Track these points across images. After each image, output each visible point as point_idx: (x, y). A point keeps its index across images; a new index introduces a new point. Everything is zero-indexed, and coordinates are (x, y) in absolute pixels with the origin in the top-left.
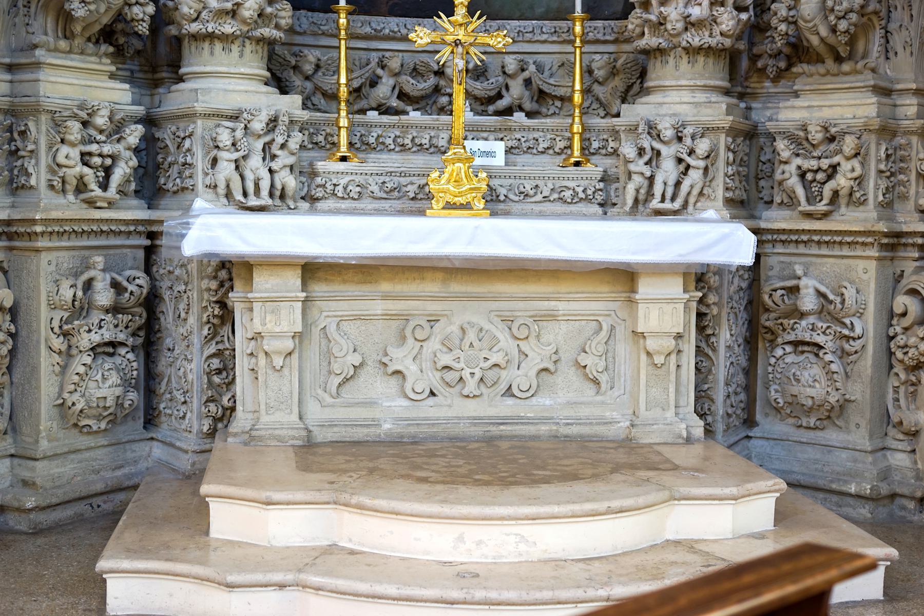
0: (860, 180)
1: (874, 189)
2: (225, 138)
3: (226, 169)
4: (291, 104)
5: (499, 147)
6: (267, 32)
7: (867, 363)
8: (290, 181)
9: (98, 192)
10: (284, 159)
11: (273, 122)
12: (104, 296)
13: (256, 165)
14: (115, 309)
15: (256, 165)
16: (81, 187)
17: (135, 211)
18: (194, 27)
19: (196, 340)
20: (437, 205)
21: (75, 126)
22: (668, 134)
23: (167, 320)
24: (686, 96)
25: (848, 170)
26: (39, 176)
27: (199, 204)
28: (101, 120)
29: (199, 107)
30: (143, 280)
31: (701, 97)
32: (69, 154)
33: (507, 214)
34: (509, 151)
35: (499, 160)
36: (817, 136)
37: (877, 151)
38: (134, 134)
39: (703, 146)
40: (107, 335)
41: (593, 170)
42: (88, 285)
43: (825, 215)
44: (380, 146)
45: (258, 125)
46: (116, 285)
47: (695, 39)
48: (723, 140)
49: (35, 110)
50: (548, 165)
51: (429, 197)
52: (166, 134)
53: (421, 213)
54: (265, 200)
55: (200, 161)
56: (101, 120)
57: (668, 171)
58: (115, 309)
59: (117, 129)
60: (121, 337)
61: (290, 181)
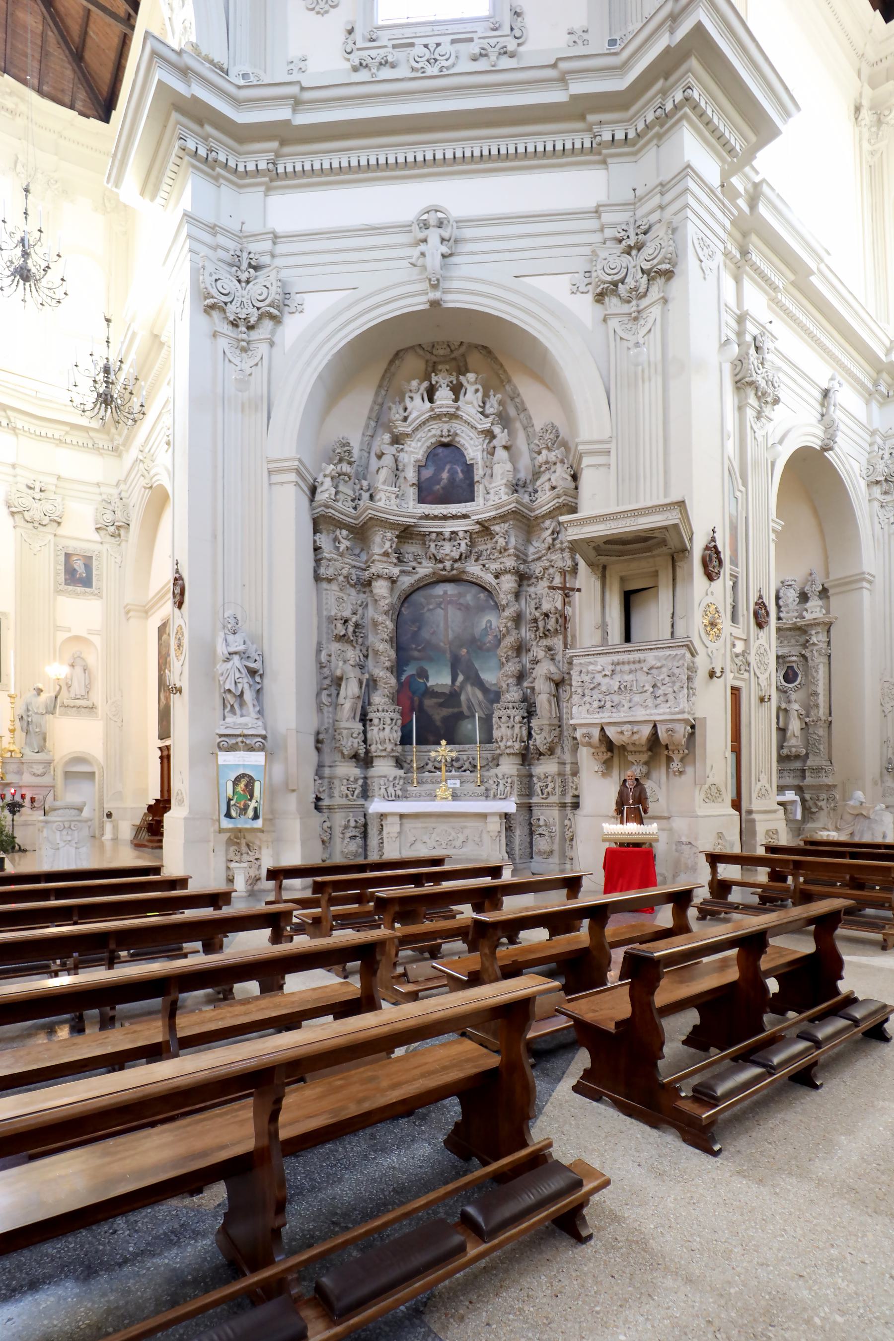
0: (554, 789)
1: (558, 791)
2: (382, 783)
3: (383, 791)
4: (401, 772)
5: (458, 782)
6: (394, 754)
7: (557, 840)
8: (399, 793)
9: (350, 797)
10: (399, 787)
11: (395, 778)
12: (352, 824)
13: (391, 790)
14: (355, 827)
15: (391, 790)
16: (347, 796)
17: (361, 801)
18: (375, 754)
19: (376, 835)
20: (438, 798)
21: (345, 781)
22: (501, 777)
23: (369, 830)
24: (507, 767)
25: (551, 785)
26: (336, 793)
27: (376, 799)
28: (352, 779)
29: (376, 774)
30: (363, 820)
31: (511, 766)
32: (344, 788)
33: (460, 800)
34: (461, 783)
35: (458, 785)
36: (543, 777)
37: (558, 780)
38: (360, 782)
39: (509, 780)
40: (353, 834)
41: (483, 788)
42: (349, 821)
43: (546, 798)
44: (426, 782)
45: (391, 779)
46: (356, 821)
47: (508, 751)
48: (515, 779)
49: (335, 777)
50: (470, 787)
51: (435, 796)
52: (369, 781)
53: (434, 800)
54: (393, 798)
55: (376, 788)
56: (352, 779)
57: (501, 787)
58: (355, 827)
59: (356, 780)
60: (357, 834)
61: (399, 793)
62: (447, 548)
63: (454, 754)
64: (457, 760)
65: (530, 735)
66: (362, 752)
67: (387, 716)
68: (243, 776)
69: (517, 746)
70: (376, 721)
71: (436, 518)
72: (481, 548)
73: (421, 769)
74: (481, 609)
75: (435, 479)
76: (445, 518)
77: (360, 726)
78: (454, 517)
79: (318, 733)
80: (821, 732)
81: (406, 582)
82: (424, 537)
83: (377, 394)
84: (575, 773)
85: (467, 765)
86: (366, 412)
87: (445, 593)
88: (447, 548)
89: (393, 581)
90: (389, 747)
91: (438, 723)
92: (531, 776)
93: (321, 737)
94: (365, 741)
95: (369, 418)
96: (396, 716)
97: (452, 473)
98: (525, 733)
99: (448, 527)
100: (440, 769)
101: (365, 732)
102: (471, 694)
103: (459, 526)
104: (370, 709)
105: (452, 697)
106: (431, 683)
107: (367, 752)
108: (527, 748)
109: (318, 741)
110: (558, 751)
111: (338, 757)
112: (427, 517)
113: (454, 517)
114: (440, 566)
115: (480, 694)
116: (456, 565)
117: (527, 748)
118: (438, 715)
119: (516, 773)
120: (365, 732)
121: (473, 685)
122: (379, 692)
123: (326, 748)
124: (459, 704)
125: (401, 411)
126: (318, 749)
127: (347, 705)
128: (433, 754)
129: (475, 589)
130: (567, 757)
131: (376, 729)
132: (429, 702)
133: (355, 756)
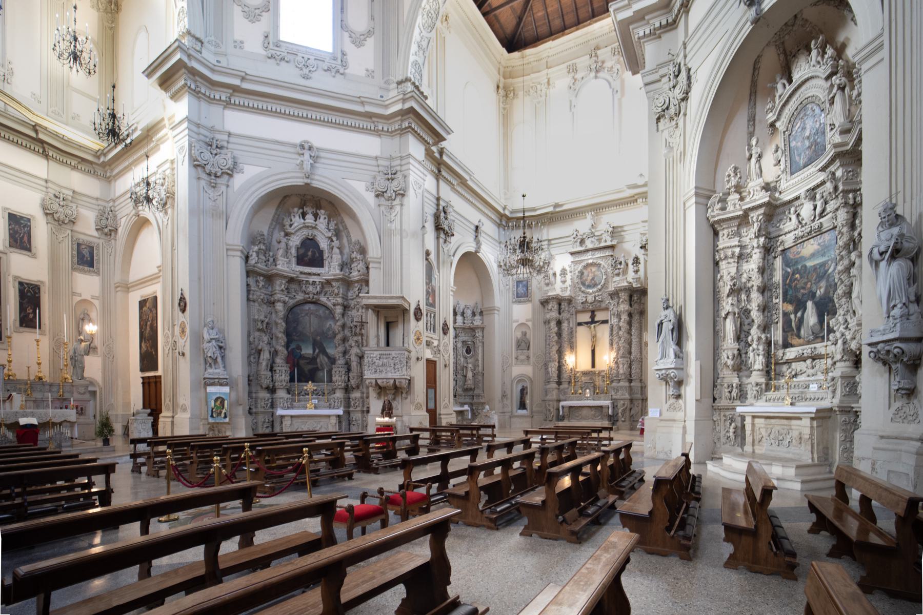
37: (361, 400)
62: (311, 288)
63: (315, 388)
64: (316, 390)
65: (349, 380)
66: (271, 386)
67: (284, 369)
68: (219, 398)
69: (343, 385)
70: (278, 371)
71: (305, 274)
72: (326, 289)
73: (299, 394)
74: (327, 318)
75: (305, 255)
76: (310, 274)
77: (269, 373)
78: (315, 274)
79: (249, 376)
80: (480, 378)
81: (292, 302)
82: (300, 282)
83: (277, 210)
84: (368, 397)
85: (320, 393)
86: (271, 217)
87: (310, 309)
88: (311, 288)
89: (284, 303)
90: (284, 384)
91: (307, 372)
92: (349, 398)
93: (251, 378)
94: (272, 381)
95: (273, 220)
96: (288, 369)
97: (314, 253)
98: (346, 379)
99: (312, 279)
100: (308, 394)
101: (272, 376)
102: (322, 359)
103: (317, 279)
104: (274, 365)
105: (313, 360)
106: (303, 352)
107: (274, 386)
108: (347, 385)
109: (249, 380)
110: (361, 387)
111: (259, 388)
112: (301, 273)
113: (315, 274)
114: (307, 296)
115: (326, 359)
116: (315, 296)
117: (347, 385)
118: (307, 368)
119: (342, 396)
120: (272, 376)
121: (323, 354)
122: (279, 357)
123: (253, 383)
124: (317, 364)
125: (289, 221)
126: (249, 385)
127: (264, 364)
128: (305, 388)
129: (324, 308)
130: (365, 390)
131: (278, 376)
132: (302, 362)
133: (267, 388)
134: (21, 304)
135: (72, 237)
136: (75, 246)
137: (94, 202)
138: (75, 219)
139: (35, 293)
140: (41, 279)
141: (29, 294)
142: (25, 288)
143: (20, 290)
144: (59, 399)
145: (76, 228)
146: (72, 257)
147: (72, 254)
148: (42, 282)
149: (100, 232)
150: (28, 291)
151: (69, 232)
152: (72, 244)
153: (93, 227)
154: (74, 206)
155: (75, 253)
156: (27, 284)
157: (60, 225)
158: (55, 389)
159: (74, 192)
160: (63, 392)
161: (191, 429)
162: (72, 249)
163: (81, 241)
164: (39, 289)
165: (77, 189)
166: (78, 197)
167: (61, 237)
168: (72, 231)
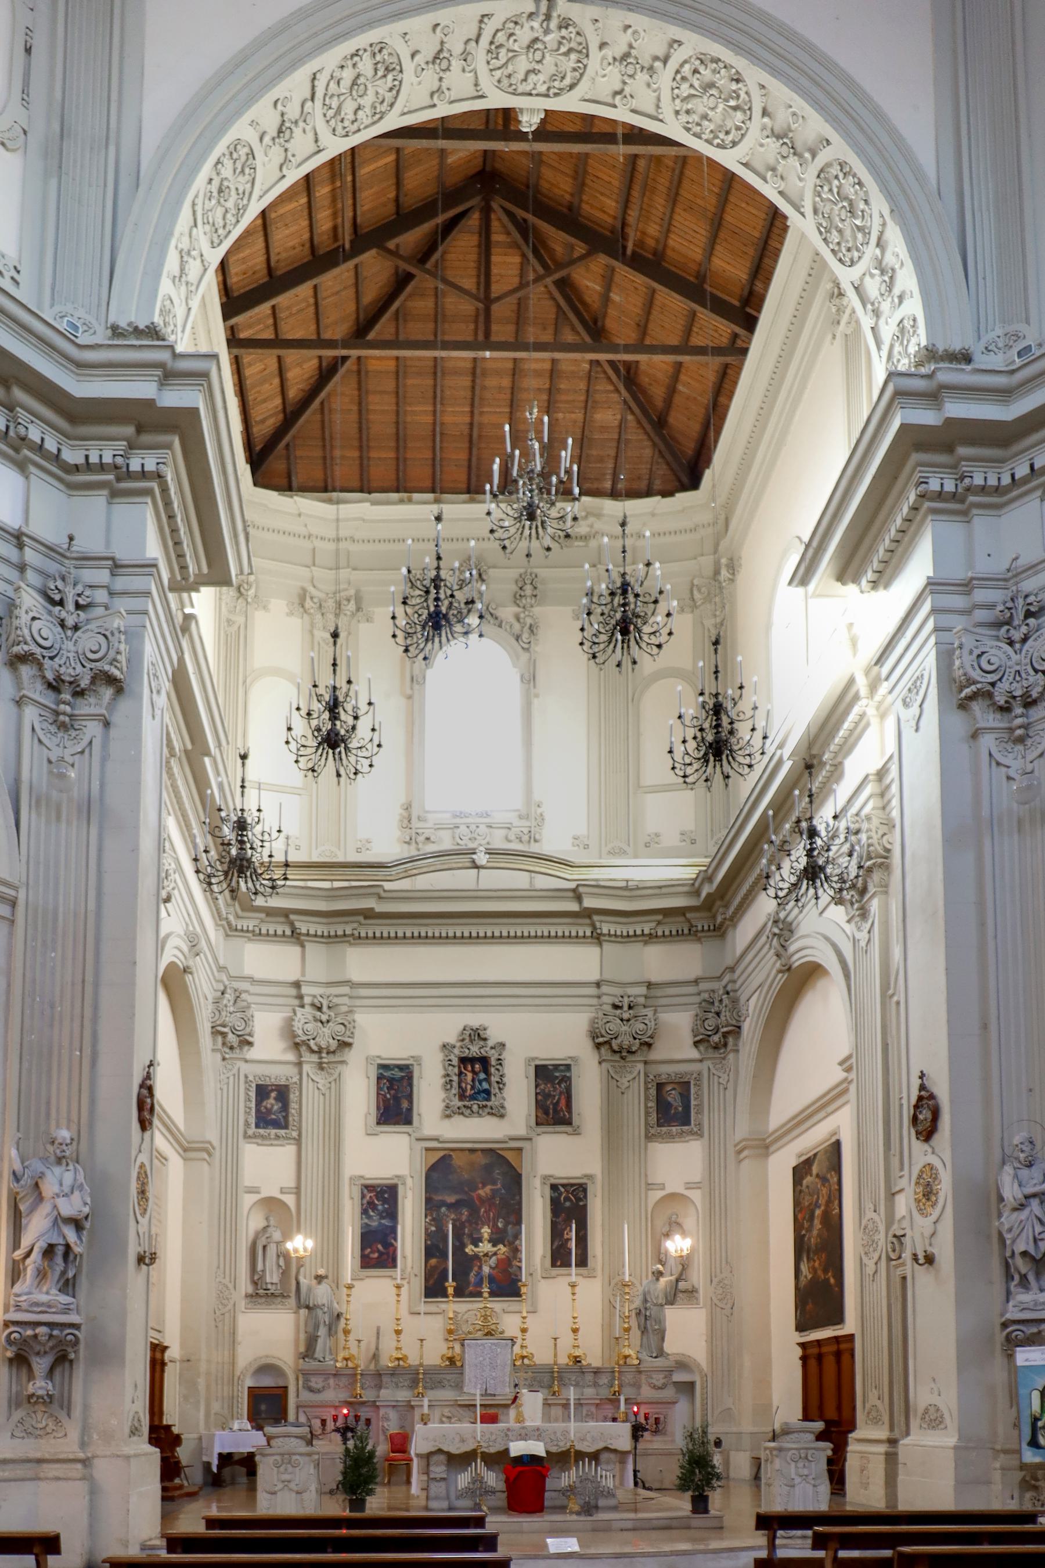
134: (554, 1225)
135: (646, 1075)
136: (653, 1092)
137: (692, 989)
138: (651, 1037)
139: (579, 1199)
140: (588, 1171)
141: (568, 1204)
142: (561, 1194)
143: (552, 1199)
144: (610, 1400)
145: (655, 1055)
146: (647, 1114)
147: (646, 1107)
148: (590, 1177)
149: (702, 1048)
150: (567, 1199)
151: (640, 1066)
152: (647, 1089)
153: (688, 1039)
154: (649, 1012)
155: (652, 1104)
156: (563, 1185)
157: (623, 1058)
158: (604, 1380)
159: (650, 985)
160: (620, 1386)
161: (961, 1484)
162: (647, 1099)
163: (663, 1079)
164: (585, 1191)
165: (654, 978)
166: (658, 992)
167: (624, 1082)
168: (646, 1063)
